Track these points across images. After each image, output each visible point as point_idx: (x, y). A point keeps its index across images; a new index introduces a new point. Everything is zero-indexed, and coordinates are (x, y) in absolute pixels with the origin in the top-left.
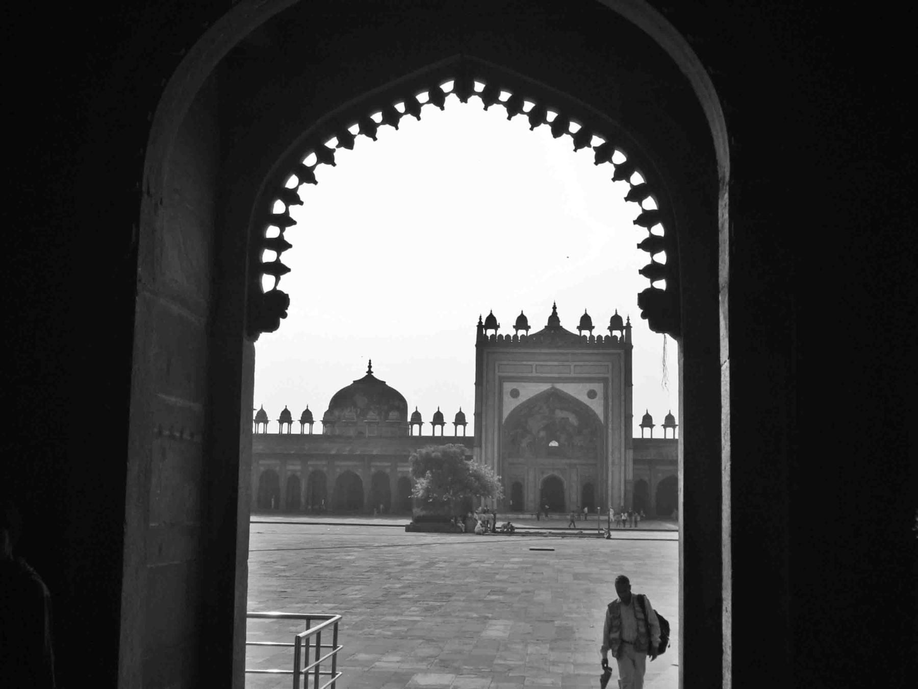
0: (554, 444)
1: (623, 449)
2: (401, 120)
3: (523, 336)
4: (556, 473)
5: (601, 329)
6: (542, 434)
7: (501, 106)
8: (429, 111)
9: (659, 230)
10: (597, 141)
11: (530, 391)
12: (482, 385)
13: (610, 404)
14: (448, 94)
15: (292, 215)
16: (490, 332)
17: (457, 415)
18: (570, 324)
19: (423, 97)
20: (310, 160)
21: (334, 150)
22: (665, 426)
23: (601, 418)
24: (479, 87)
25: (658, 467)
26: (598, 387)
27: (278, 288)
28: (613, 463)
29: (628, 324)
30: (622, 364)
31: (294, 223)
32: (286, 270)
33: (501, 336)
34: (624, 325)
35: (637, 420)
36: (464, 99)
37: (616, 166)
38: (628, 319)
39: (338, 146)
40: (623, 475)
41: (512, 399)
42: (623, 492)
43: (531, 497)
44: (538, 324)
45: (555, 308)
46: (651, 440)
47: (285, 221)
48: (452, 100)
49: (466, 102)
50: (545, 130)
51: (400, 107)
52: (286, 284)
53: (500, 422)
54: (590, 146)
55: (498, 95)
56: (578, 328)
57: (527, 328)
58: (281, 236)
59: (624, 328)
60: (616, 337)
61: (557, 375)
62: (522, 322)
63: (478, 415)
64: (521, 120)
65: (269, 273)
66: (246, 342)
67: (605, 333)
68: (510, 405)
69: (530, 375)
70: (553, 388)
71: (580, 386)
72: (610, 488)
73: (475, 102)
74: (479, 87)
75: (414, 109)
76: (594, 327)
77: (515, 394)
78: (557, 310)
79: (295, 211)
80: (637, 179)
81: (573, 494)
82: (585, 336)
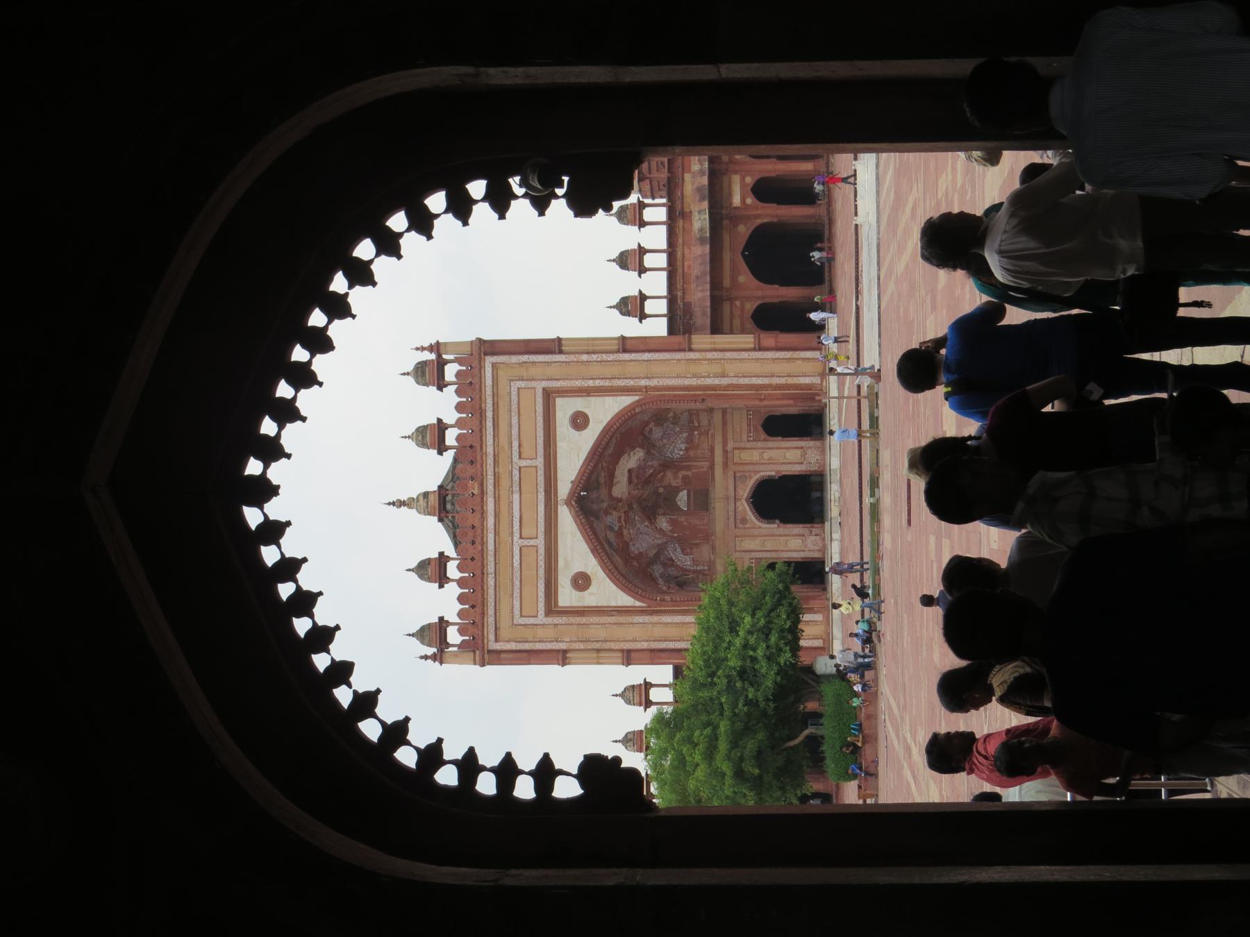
0: (682, 499)
1: (691, 355)
2: (305, 588)
3: (460, 568)
4: (746, 490)
5: (442, 405)
7: (283, 433)
8: (291, 545)
9: (477, 188)
10: (339, 283)
11: (575, 552)
12: (565, 652)
13: (598, 383)
14: (265, 516)
15: (459, 755)
16: (454, 636)
17: (628, 702)
18: (433, 469)
19: (270, 555)
20: (371, 729)
21: (355, 692)
22: (642, 270)
23: (627, 400)
24: (254, 467)
25: (727, 282)
27: (575, 772)
29: (431, 348)
30: (514, 359)
31: (471, 751)
32: (546, 762)
33: (461, 614)
34: (433, 356)
35: (631, 327)
36: (273, 491)
37: (378, 255)
38: (423, 349)
39: (350, 686)
40: (745, 355)
41: (592, 589)
43: (795, 543)
44: (433, 538)
45: (400, 504)
46: (672, 299)
47: (469, 766)
48: (275, 509)
49: (278, 487)
50: (321, 364)
51: (285, 590)
52: (567, 760)
53: (641, 612)
54: (347, 294)
55: (266, 436)
56: (440, 453)
57: (443, 559)
58: (492, 770)
59: (439, 356)
60: (458, 374)
61: (541, 496)
62: (433, 570)
63: (629, 658)
64: (306, 400)
65: (551, 787)
66: (663, 813)
67: (450, 397)
68: (606, 591)
69: (542, 551)
70: (568, 503)
71: (562, 446)
73: (276, 472)
74: (254, 467)
75: (289, 568)
76: (439, 420)
77: (582, 582)
78: (404, 498)
79: (452, 751)
80: (398, 221)
81: (788, 457)
82: (458, 438)
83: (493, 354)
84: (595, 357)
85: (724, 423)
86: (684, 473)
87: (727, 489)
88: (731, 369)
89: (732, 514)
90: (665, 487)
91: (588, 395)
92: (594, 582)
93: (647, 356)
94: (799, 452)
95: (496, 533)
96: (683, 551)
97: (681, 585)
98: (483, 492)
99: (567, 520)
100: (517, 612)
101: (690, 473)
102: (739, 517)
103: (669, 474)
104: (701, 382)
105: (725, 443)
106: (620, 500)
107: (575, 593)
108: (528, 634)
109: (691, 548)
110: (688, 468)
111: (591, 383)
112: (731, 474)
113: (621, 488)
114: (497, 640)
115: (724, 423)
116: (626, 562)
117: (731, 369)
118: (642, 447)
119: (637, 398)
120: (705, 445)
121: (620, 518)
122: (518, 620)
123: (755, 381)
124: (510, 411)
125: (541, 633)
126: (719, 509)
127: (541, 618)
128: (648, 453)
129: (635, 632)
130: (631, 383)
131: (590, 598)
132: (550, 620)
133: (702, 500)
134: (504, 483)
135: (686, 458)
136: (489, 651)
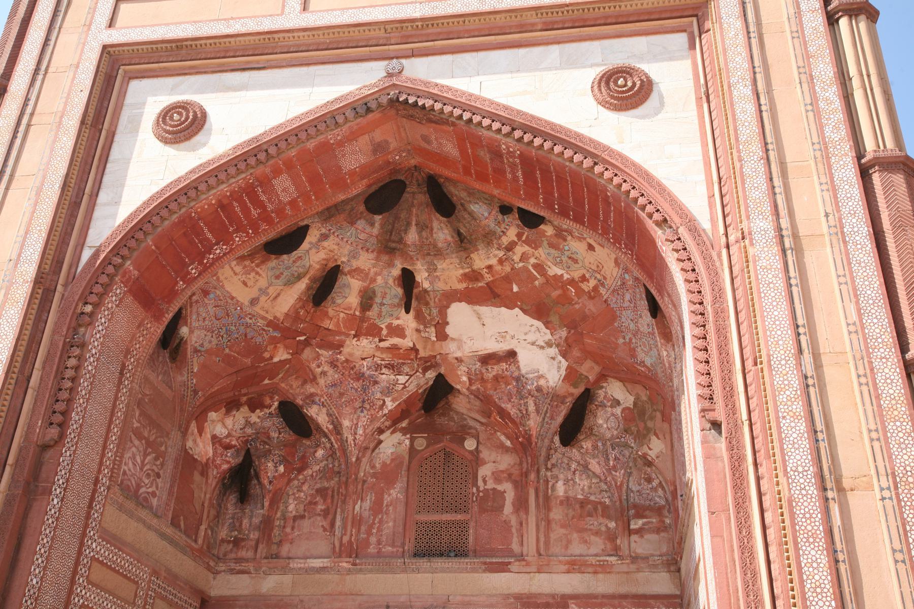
6: (393, 444)
28: (829, 483)
84: (831, 95)
86: (510, 495)
96: (322, 492)
97: (241, 479)
101: (508, 508)
103: (506, 461)
106: (442, 336)
109: (325, 513)
110: (521, 504)
116: (285, 331)
118: (571, 376)
119: (705, 223)
121: (399, 332)
128: (556, 397)
133: (437, 545)
135: (546, 502)
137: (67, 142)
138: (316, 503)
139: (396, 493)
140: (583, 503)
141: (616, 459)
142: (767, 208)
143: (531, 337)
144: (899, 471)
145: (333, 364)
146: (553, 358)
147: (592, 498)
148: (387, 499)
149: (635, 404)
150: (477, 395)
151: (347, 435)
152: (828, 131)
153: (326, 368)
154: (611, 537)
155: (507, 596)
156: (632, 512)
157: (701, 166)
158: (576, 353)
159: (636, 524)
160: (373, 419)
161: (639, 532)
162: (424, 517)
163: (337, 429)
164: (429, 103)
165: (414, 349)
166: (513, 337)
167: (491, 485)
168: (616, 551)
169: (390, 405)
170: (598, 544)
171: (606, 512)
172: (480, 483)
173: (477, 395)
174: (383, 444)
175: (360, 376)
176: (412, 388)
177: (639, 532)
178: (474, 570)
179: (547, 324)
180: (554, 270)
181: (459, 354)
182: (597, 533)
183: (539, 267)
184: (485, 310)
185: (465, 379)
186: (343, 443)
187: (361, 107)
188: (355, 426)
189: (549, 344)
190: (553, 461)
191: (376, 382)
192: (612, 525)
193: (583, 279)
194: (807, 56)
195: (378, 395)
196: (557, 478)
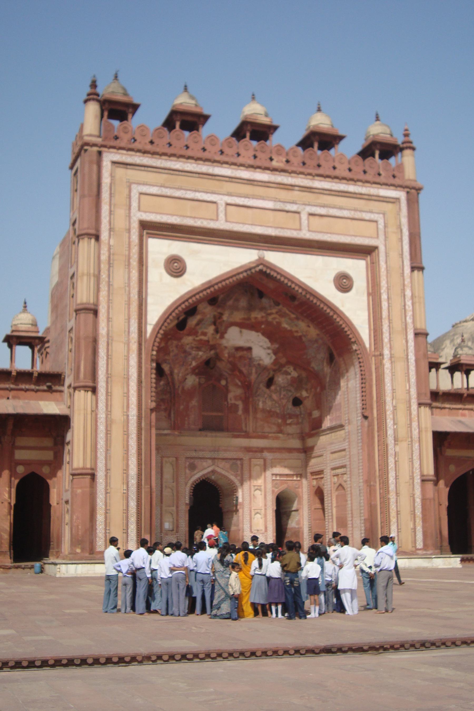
1: (414, 406)
6: (191, 381)
13: (385, 305)
26: (356, 267)
28: (396, 440)
30: (404, 221)
40: (417, 464)
41: (168, 278)
42: (418, 501)
70: (261, 261)
72: (392, 497)
77: (176, 267)
83: (409, 201)
84: (409, 303)
85: (290, 450)
87: (225, 451)
88: (402, 448)
89: (201, 454)
90: (226, 387)
91: (369, 294)
92: (175, 280)
93: (412, 357)
94: (262, 527)
95: (231, 179)
98: (275, 170)
99: (240, 258)
100: (145, 189)
101: (240, 412)
102: (196, 462)
104: (389, 413)
105: (270, 450)
106: (222, 337)
107: (162, 258)
108: (120, 198)
109: (165, 410)
110: (246, 410)
111: (384, 297)
112: (240, 455)
113: (235, 337)
114: (114, 163)
115: (290, 450)
117: (402, 448)
118: (275, 362)
119: (367, 345)
120: (267, 429)
121: (204, 334)
122: (136, 190)
123: (392, 475)
124: (355, 210)
125: (120, 213)
126: (207, 440)
127: (138, 216)
128: (265, 368)
129: (119, 320)
130: (386, 340)
131: (157, 274)
132: (135, 226)
133: (211, 426)
134: (283, 194)
135: (256, 410)
136: (100, 153)
137: (135, 274)
138: (161, 406)
139: (194, 403)
140: (270, 412)
141: (284, 395)
142: (388, 345)
143: (261, 344)
144: (413, 437)
145: (177, 347)
146: (269, 354)
147: (273, 410)
148: (191, 405)
149: (298, 377)
150: (230, 362)
151: (176, 377)
152: (408, 318)
153: (174, 349)
154: (279, 426)
155: (241, 448)
156: (288, 416)
157: (367, 321)
158: (280, 355)
159: (289, 421)
160: (187, 369)
161: (290, 424)
162: (205, 414)
163: (172, 373)
164: (275, 275)
165: (208, 341)
166: (253, 342)
167: (233, 402)
168: (281, 432)
169: (194, 364)
170: (275, 428)
171: (277, 415)
172: (229, 400)
173: (230, 362)
174: (187, 381)
175: (185, 352)
176: (205, 357)
177: (290, 424)
178: (228, 437)
179: (270, 341)
180: (285, 325)
181: (226, 345)
182: (274, 424)
183: (279, 324)
184: (245, 331)
185: (226, 355)
186: (173, 379)
187: (248, 269)
188: (178, 373)
189: (269, 348)
190: (258, 393)
191: (190, 354)
192: (280, 421)
193: (297, 332)
194: (404, 285)
195: (190, 360)
196: (259, 400)
